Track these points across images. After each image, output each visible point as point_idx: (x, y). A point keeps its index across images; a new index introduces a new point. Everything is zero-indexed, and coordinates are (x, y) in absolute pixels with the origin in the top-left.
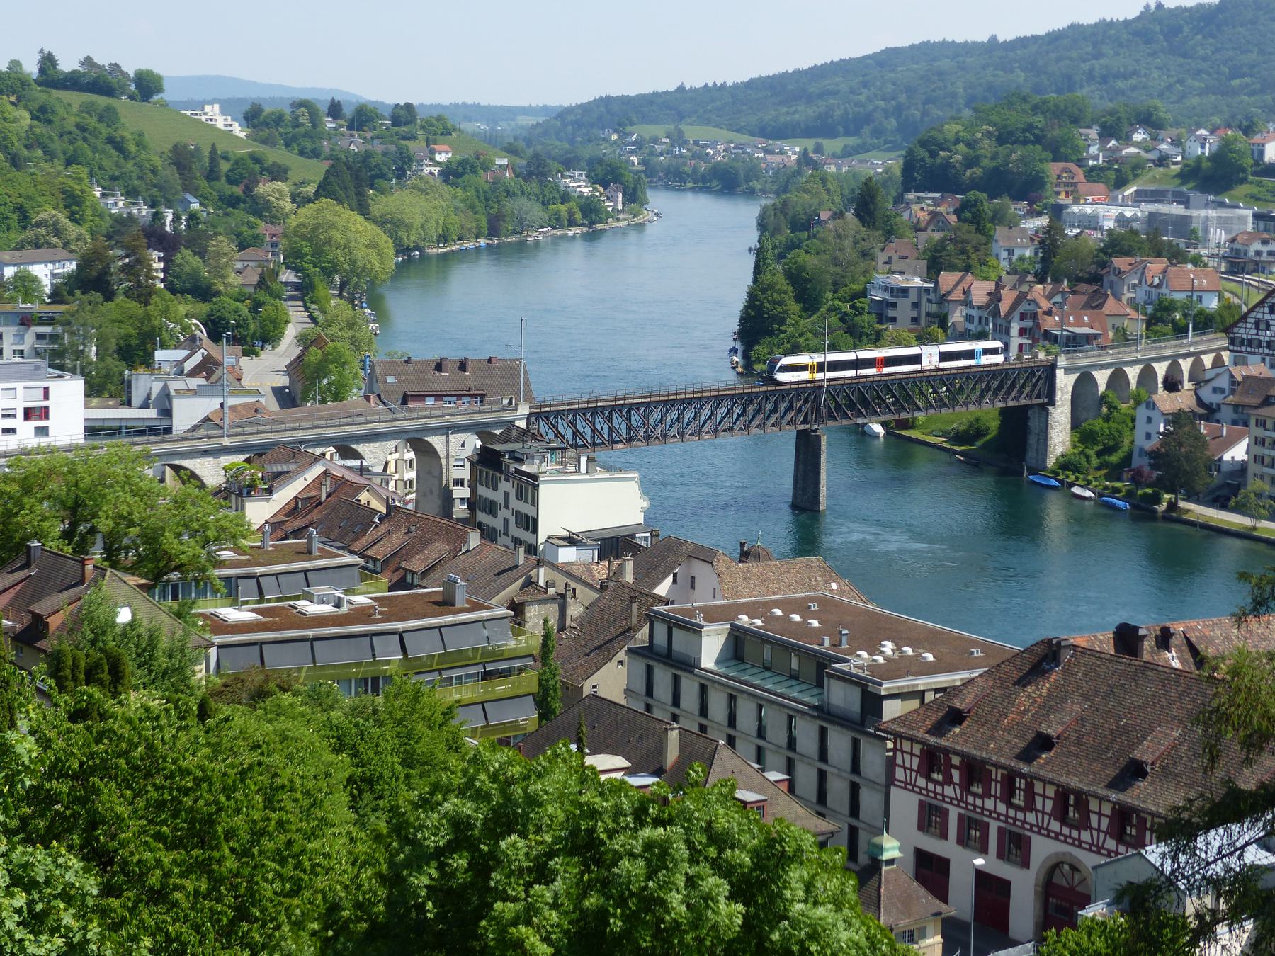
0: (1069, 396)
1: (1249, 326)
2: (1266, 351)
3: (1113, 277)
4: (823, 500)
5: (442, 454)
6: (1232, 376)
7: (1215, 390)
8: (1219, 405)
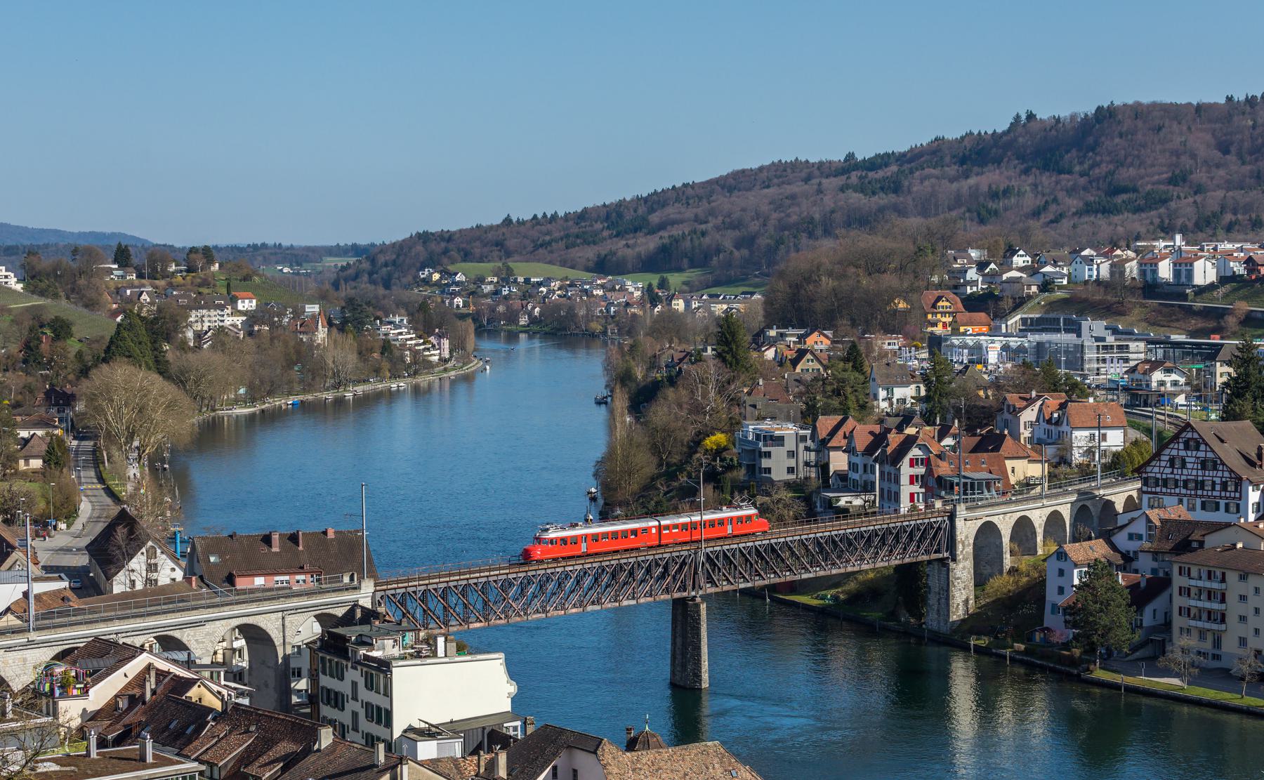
0: (970, 549)
1: (1163, 464)
2: (1183, 491)
3: (1006, 415)
4: (705, 676)
5: (278, 642)
6: (1149, 520)
7: (1131, 537)
8: (1135, 552)
